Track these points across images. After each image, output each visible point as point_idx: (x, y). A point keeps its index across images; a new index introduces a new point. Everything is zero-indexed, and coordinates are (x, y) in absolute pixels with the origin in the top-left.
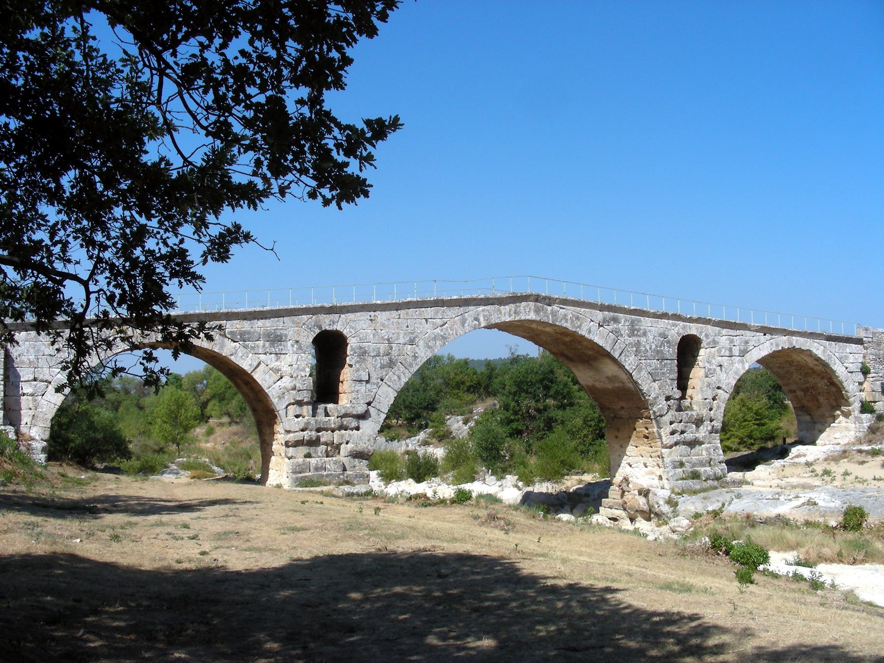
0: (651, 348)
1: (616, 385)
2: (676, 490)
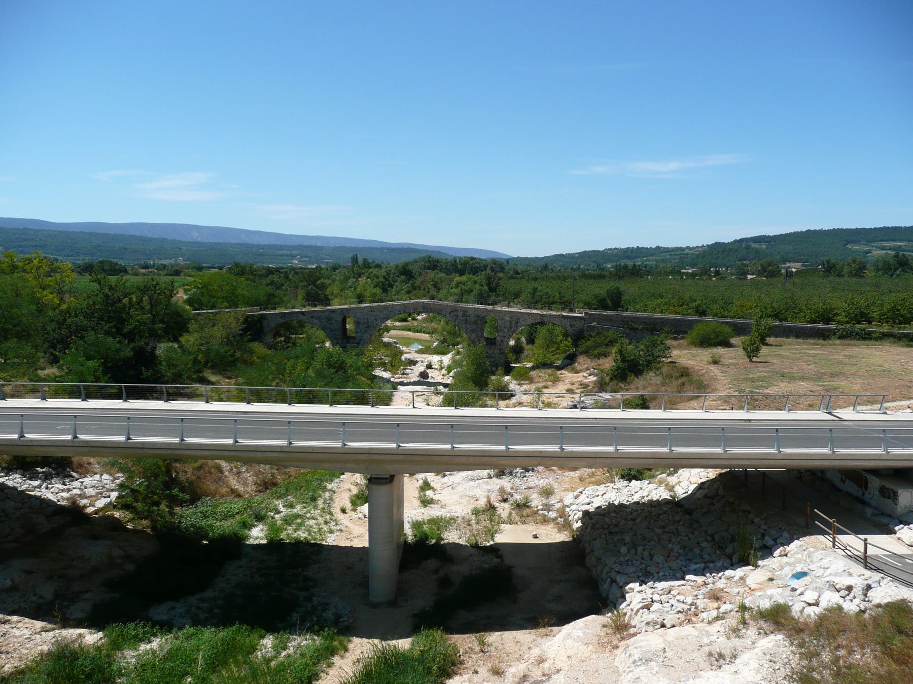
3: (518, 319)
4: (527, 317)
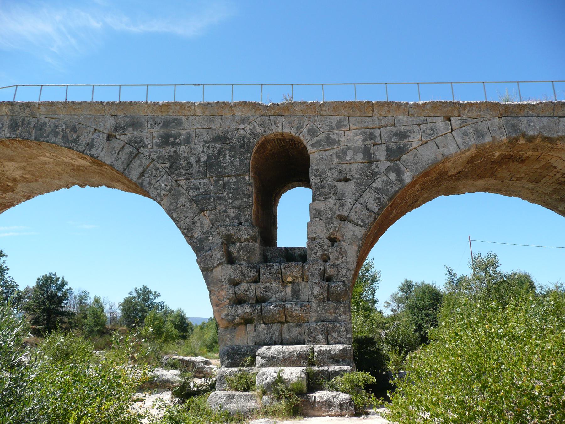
0: (198, 161)
3: (402, 135)
4: (441, 126)
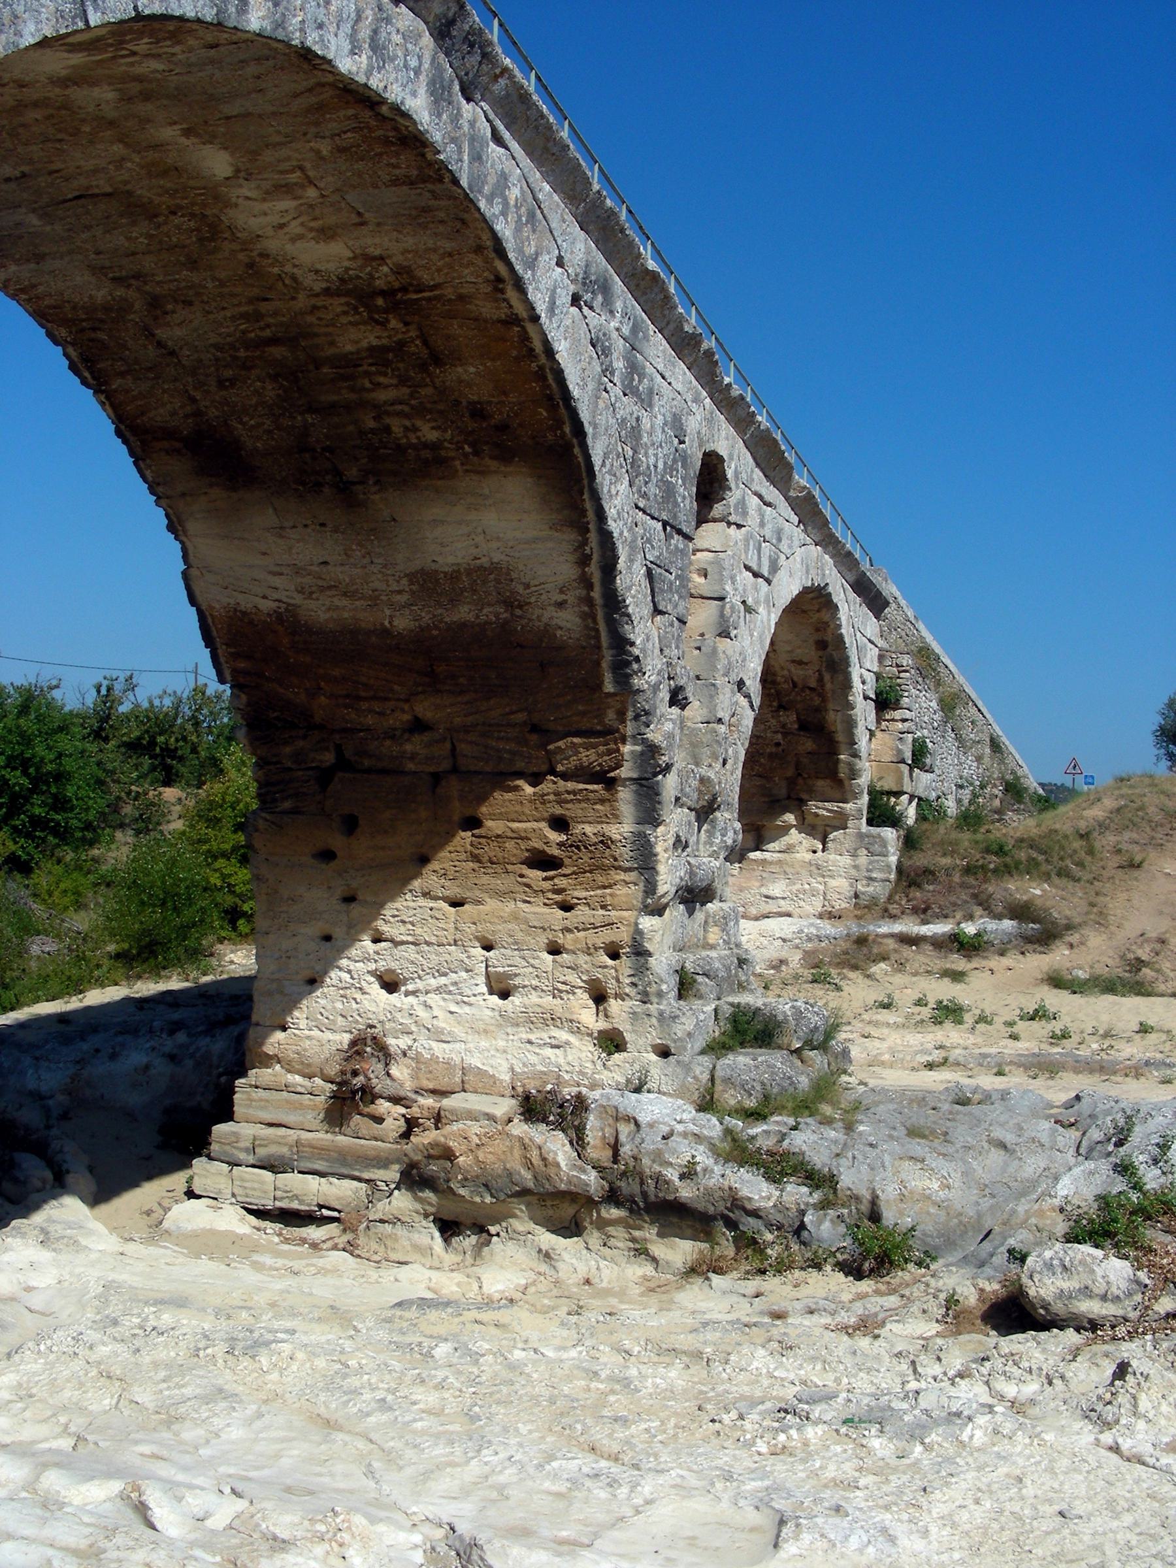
0: (656, 467)
1: (464, 613)
2: (730, 1098)
